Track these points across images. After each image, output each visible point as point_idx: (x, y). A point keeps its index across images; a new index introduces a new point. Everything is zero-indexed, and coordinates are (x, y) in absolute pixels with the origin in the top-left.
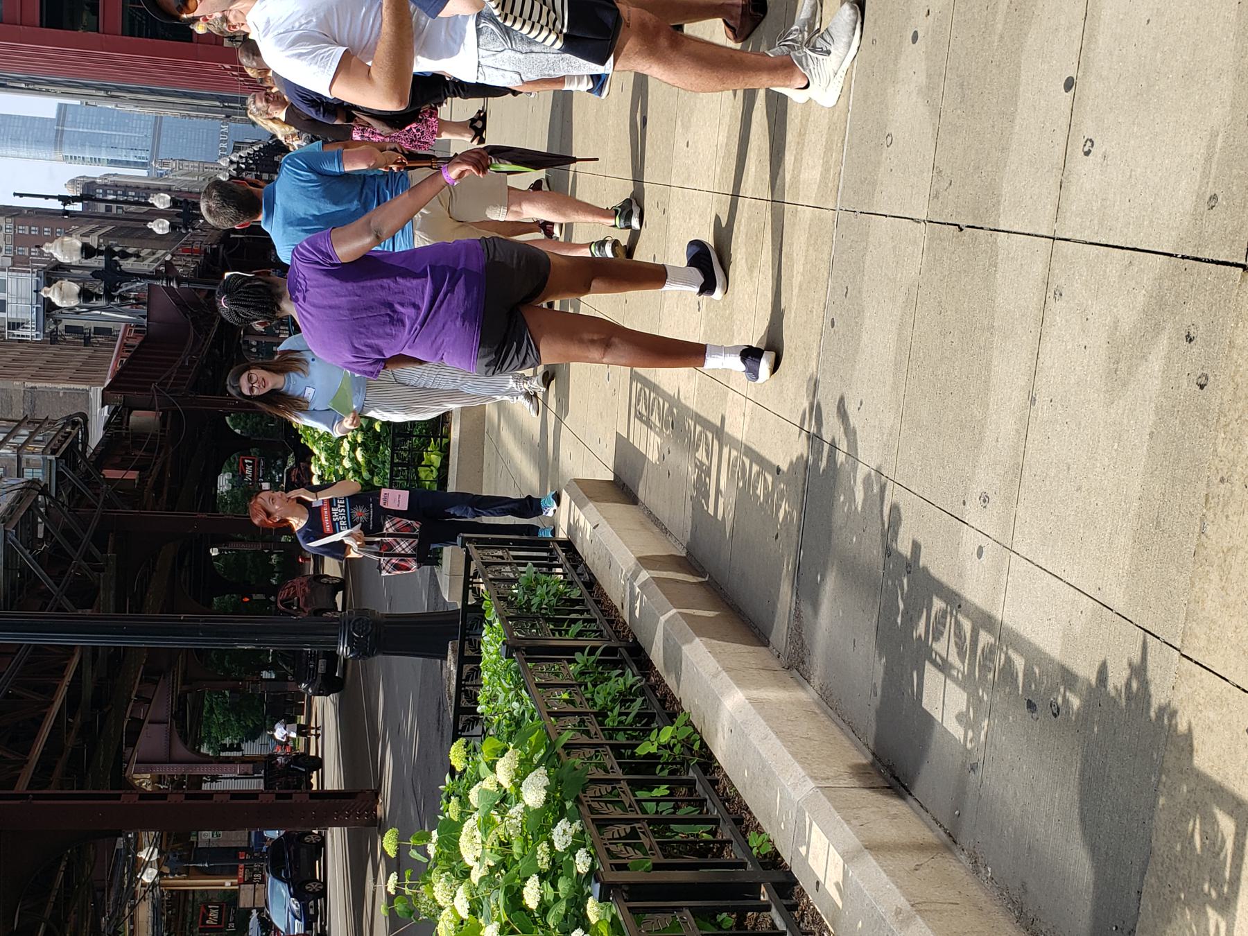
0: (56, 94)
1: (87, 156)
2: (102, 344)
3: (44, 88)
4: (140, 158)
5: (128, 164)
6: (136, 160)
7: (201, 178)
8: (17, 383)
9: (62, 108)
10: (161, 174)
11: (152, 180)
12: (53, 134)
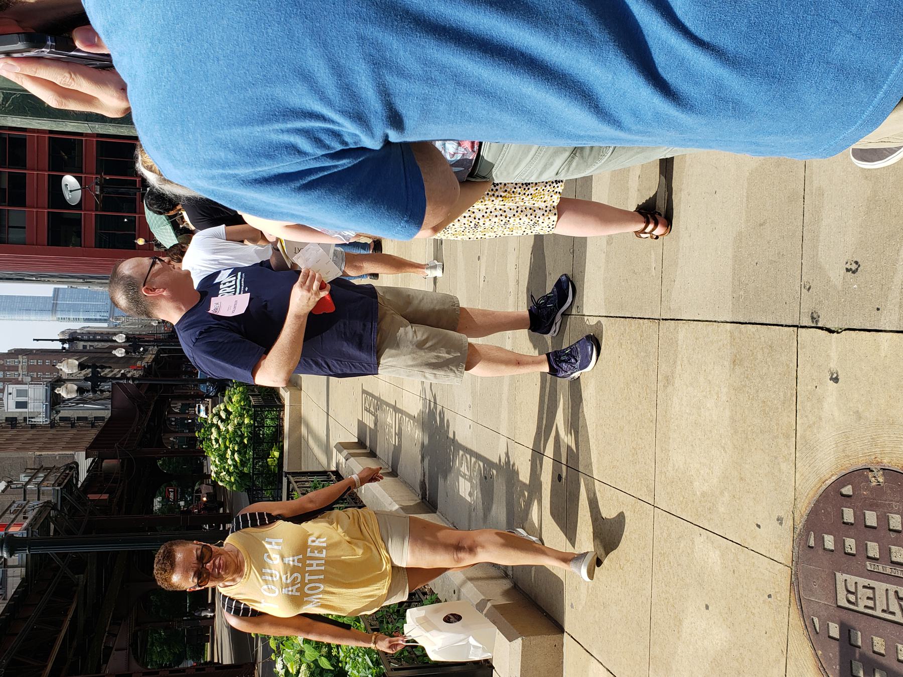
0: (53, 282)
1: (71, 317)
2: (82, 427)
3: (47, 279)
4: (103, 316)
5: (96, 320)
6: (100, 318)
7: (140, 326)
8: (31, 453)
9: (56, 291)
10: (116, 325)
11: (111, 328)
12: (51, 306)
